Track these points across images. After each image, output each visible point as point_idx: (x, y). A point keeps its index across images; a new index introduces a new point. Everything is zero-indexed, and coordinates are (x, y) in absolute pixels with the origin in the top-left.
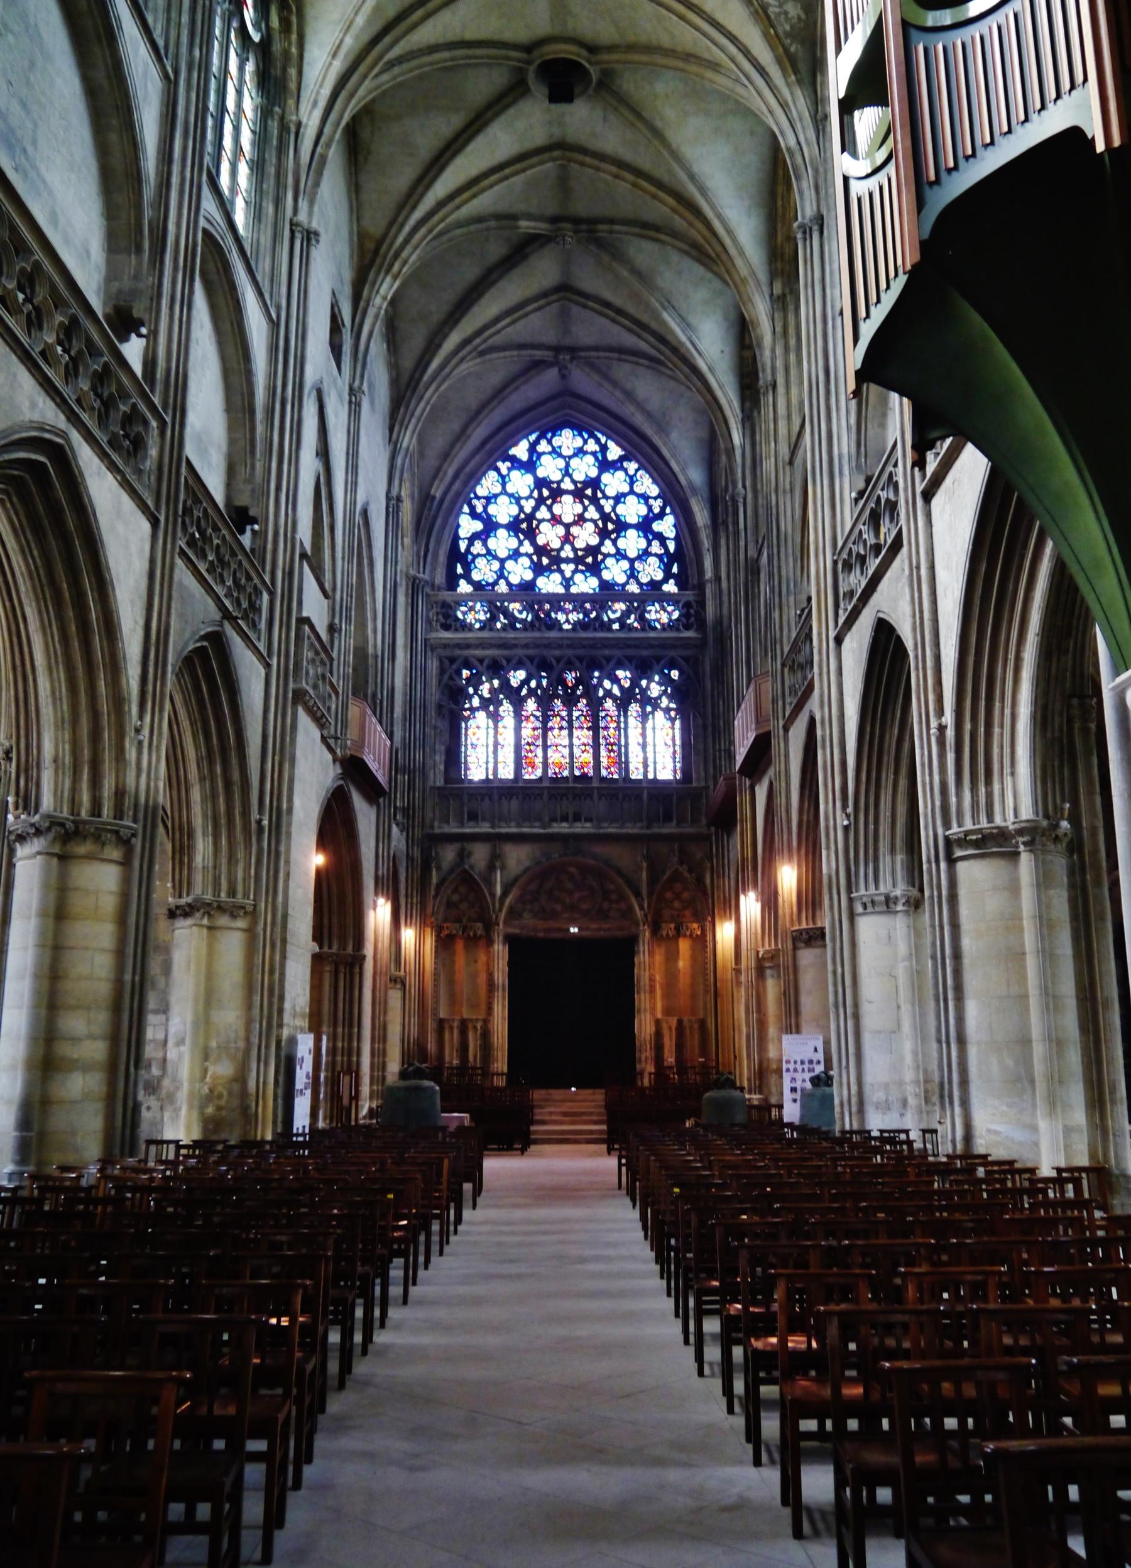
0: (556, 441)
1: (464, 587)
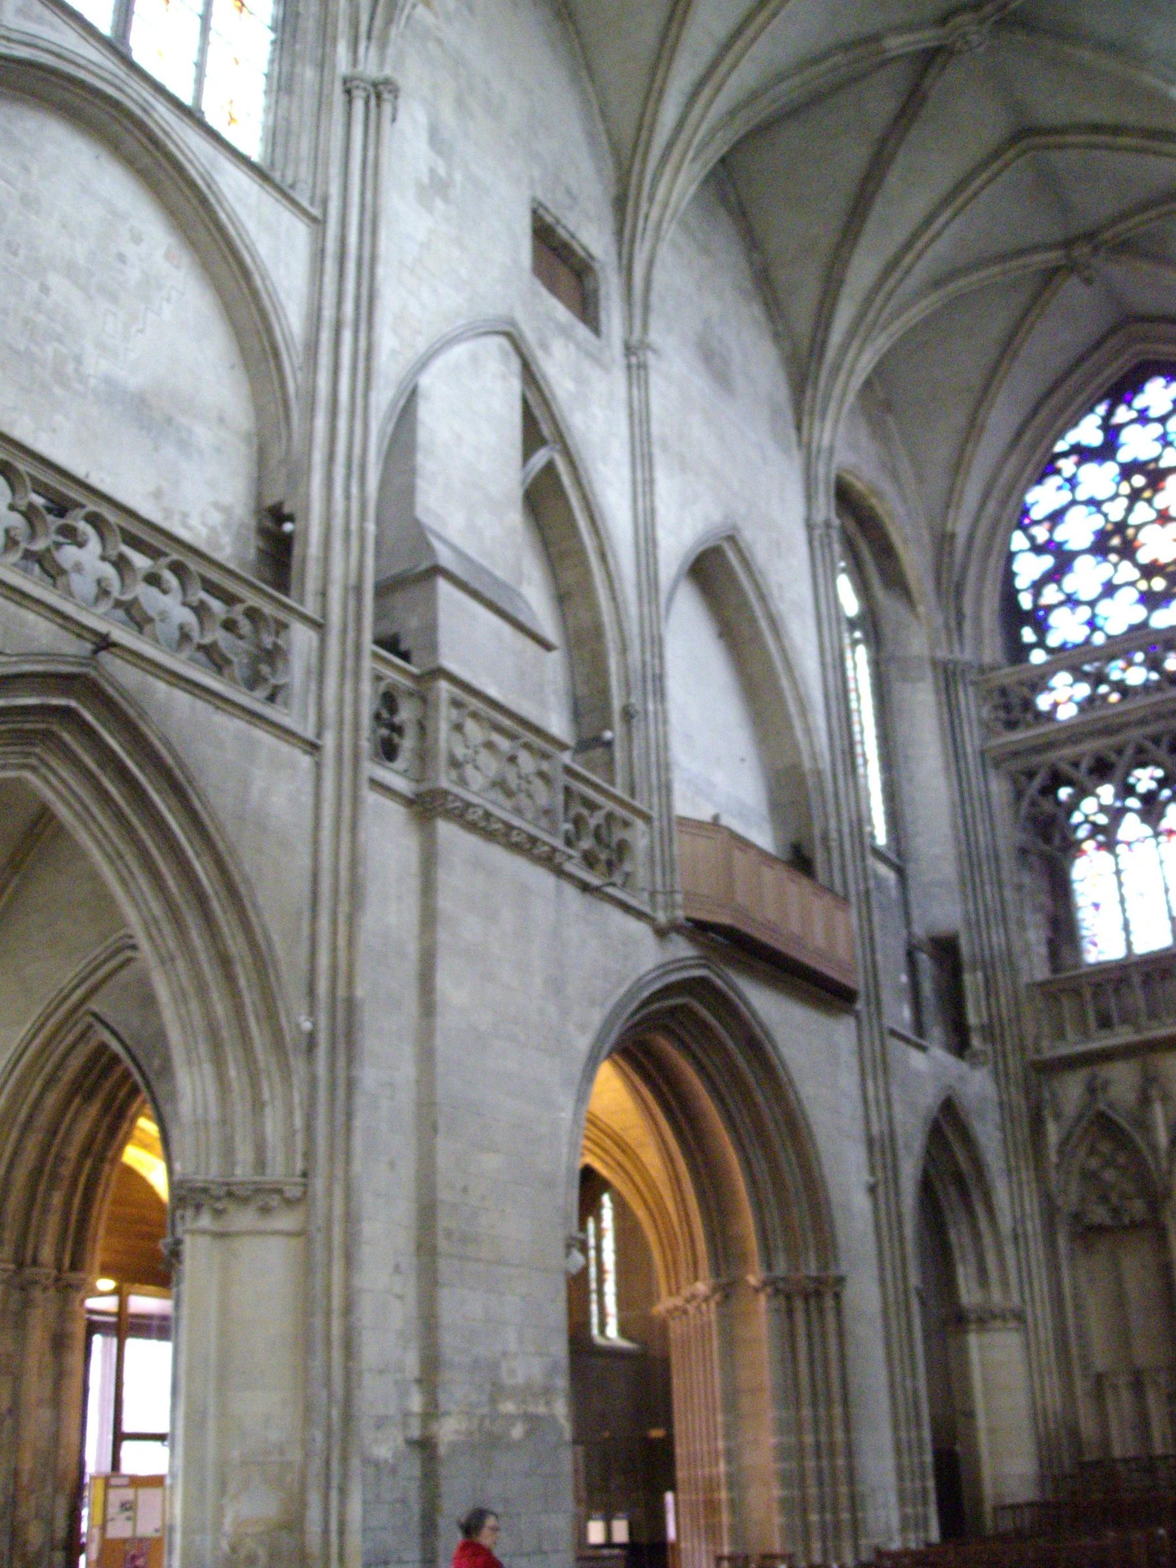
0: (1139, 402)
1: (1038, 657)
